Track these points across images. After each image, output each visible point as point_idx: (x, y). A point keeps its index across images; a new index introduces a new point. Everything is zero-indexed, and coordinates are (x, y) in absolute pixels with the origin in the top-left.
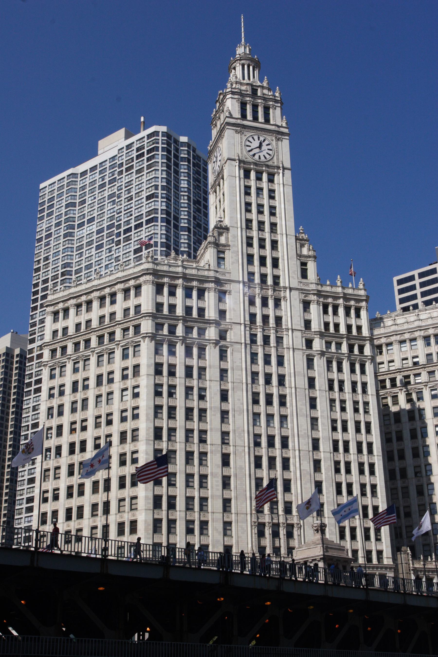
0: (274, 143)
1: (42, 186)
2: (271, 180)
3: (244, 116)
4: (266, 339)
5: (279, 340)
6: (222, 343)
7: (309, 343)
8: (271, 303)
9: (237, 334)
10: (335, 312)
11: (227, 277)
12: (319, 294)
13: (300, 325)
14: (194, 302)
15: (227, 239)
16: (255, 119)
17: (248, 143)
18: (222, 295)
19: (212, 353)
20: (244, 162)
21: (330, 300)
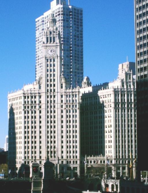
0: (55, 49)
1: (36, 20)
2: (54, 61)
3: (47, 41)
4: (51, 107)
5: (54, 107)
6: (40, 109)
7: (62, 106)
8: (53, 97)
9: (43, 106)
10: (70, 97)
11: (41, 92)
12: (65, 92)
13: (59, 101)
14: (33, 100)
15: (42, 81)
16: (51, 41)
17: (48, 51)
18: (40, 97)
19: (38, 112)
20: (47, 57)
21: (68, 94)
